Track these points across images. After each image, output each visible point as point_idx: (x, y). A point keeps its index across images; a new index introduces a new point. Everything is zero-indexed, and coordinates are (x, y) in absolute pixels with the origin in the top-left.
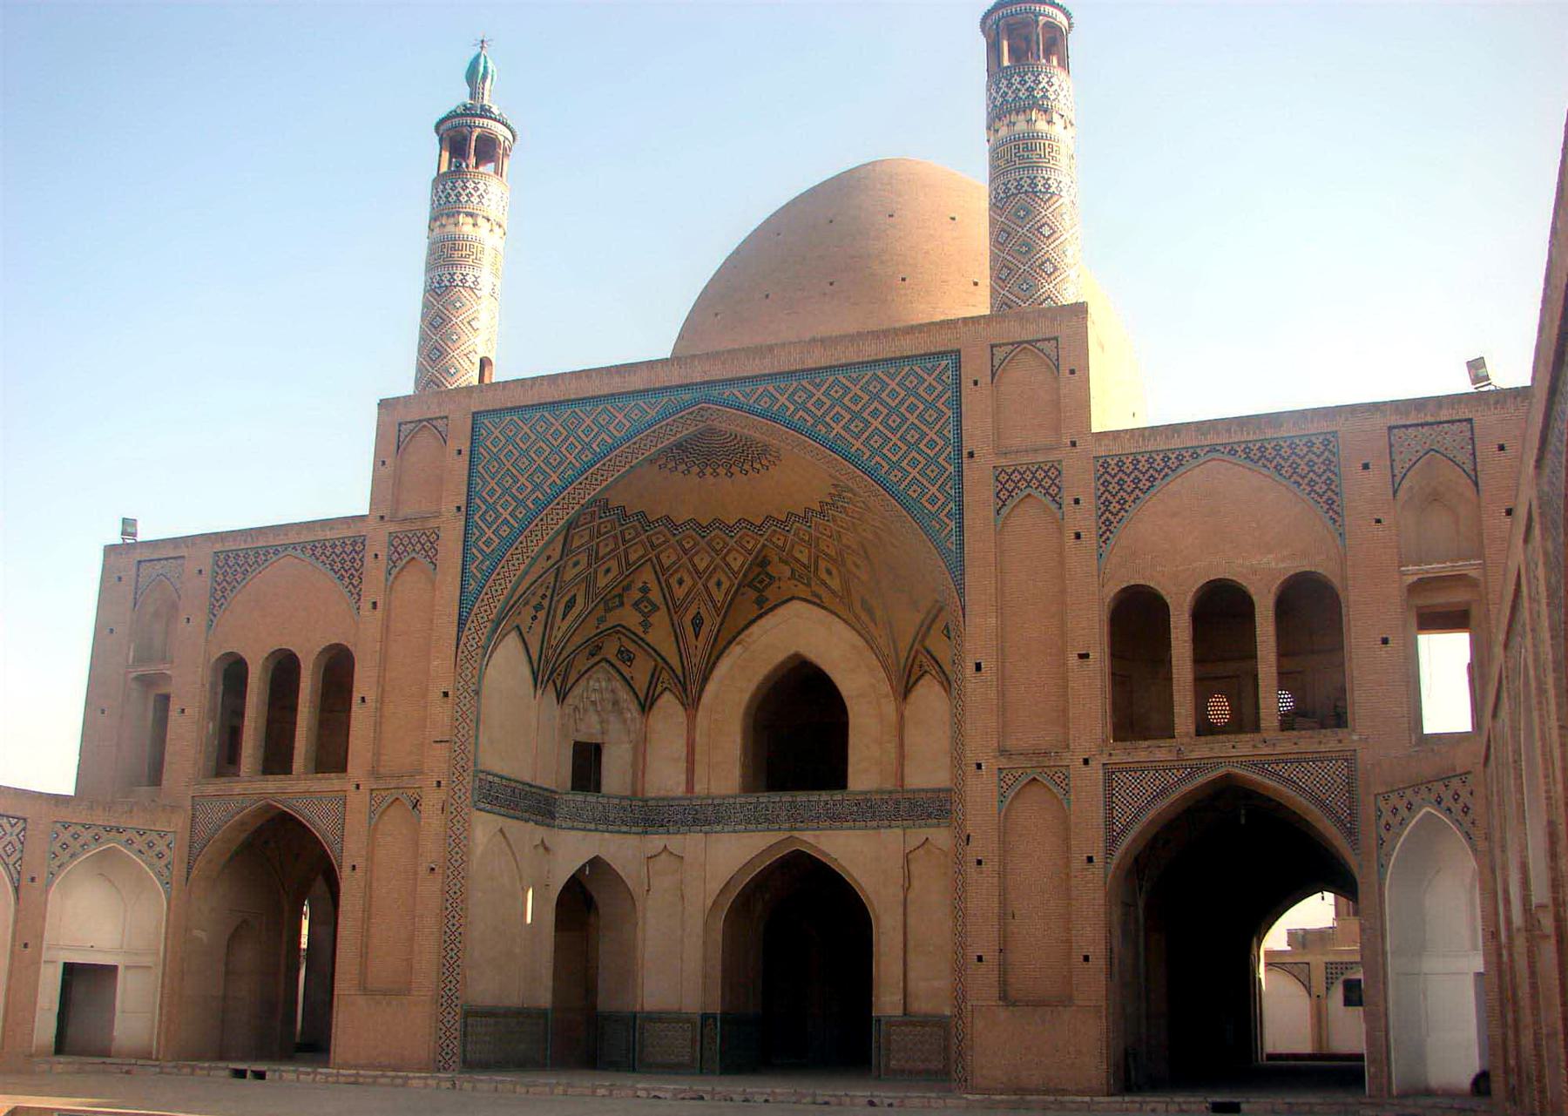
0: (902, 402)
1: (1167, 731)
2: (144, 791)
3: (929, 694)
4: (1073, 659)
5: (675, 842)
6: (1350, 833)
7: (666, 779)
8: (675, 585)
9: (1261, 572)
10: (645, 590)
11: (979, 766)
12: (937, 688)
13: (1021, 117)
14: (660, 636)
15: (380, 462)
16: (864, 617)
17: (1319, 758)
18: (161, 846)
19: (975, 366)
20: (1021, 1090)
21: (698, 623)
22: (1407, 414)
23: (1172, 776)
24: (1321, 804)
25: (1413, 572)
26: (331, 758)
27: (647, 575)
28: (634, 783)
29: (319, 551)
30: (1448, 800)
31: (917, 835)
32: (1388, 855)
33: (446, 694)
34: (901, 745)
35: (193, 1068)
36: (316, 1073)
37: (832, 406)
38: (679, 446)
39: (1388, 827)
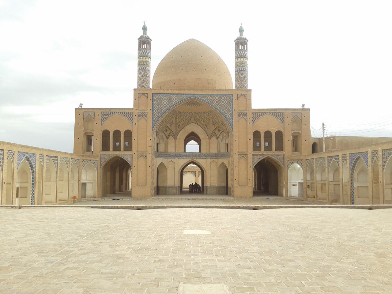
0: (224, 101)
1: (260, 150)
2: (88, 153)
3: (214, 139)
4: (248, 140)
5: (173, 160)
6: (284, 165)
7: (171, 150)
8: (177, 120)
9: (273, 130)
10: (172, 121)
11: (235, 154)
12: (215, 138)
13: (242, 58)
14: (173, 128)
15: (135, 100)
16: (205, 127)
17: (280, 155)
18: (96, 162)
19: (235, 97)
20: (242, 197)
21: (179, 126)
22: (293, 111)
23: (261, 156)
24: (280, 161)
25: (293, 132)
26: (129, 148)
27: (174, 119)
28: (165, 150)
29: (124, 114)
30: (299, 162)
31: (212, 160)
32: (289, 168)
33: (150, 139)
34: (210, 146)
35: (105, 199)
36: (129, 199)
37: (213, 100)
38: (187, 103)
39: (289, 164)
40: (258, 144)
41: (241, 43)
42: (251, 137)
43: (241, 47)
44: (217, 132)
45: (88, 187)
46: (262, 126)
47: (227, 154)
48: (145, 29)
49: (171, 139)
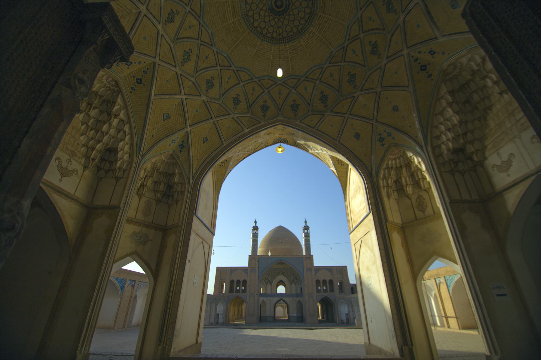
3: (293, 285)
5: (270, 298)
7: (269, 292)
15: (249, 261)
19: (304, 259)
26: (244, 291)
40: (319, 288)
41: (306, 228)
42: (314, 283)
43: (306, 231)
44: (295, 280)
45: (220, 316)
46: (321, 277)
47: (300, 294)
48: (256, 222)
49: (269, 284)
